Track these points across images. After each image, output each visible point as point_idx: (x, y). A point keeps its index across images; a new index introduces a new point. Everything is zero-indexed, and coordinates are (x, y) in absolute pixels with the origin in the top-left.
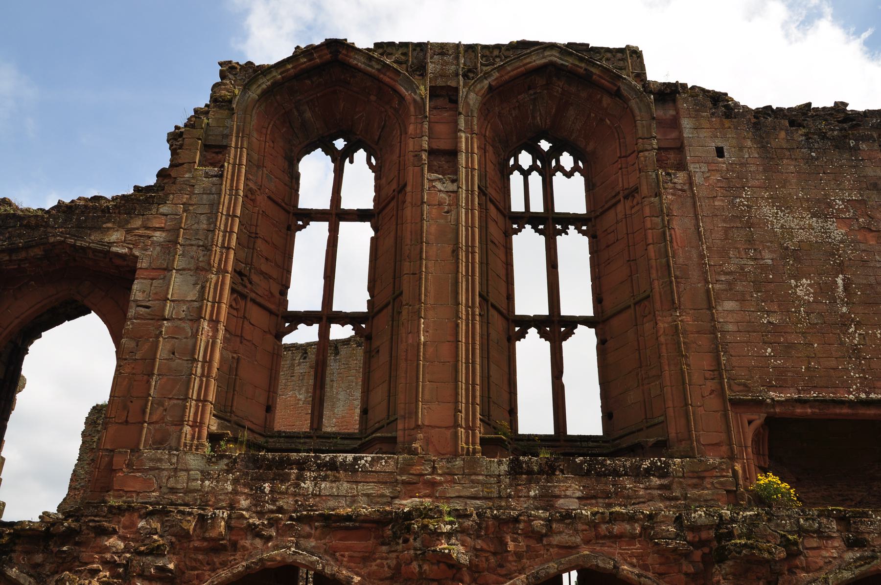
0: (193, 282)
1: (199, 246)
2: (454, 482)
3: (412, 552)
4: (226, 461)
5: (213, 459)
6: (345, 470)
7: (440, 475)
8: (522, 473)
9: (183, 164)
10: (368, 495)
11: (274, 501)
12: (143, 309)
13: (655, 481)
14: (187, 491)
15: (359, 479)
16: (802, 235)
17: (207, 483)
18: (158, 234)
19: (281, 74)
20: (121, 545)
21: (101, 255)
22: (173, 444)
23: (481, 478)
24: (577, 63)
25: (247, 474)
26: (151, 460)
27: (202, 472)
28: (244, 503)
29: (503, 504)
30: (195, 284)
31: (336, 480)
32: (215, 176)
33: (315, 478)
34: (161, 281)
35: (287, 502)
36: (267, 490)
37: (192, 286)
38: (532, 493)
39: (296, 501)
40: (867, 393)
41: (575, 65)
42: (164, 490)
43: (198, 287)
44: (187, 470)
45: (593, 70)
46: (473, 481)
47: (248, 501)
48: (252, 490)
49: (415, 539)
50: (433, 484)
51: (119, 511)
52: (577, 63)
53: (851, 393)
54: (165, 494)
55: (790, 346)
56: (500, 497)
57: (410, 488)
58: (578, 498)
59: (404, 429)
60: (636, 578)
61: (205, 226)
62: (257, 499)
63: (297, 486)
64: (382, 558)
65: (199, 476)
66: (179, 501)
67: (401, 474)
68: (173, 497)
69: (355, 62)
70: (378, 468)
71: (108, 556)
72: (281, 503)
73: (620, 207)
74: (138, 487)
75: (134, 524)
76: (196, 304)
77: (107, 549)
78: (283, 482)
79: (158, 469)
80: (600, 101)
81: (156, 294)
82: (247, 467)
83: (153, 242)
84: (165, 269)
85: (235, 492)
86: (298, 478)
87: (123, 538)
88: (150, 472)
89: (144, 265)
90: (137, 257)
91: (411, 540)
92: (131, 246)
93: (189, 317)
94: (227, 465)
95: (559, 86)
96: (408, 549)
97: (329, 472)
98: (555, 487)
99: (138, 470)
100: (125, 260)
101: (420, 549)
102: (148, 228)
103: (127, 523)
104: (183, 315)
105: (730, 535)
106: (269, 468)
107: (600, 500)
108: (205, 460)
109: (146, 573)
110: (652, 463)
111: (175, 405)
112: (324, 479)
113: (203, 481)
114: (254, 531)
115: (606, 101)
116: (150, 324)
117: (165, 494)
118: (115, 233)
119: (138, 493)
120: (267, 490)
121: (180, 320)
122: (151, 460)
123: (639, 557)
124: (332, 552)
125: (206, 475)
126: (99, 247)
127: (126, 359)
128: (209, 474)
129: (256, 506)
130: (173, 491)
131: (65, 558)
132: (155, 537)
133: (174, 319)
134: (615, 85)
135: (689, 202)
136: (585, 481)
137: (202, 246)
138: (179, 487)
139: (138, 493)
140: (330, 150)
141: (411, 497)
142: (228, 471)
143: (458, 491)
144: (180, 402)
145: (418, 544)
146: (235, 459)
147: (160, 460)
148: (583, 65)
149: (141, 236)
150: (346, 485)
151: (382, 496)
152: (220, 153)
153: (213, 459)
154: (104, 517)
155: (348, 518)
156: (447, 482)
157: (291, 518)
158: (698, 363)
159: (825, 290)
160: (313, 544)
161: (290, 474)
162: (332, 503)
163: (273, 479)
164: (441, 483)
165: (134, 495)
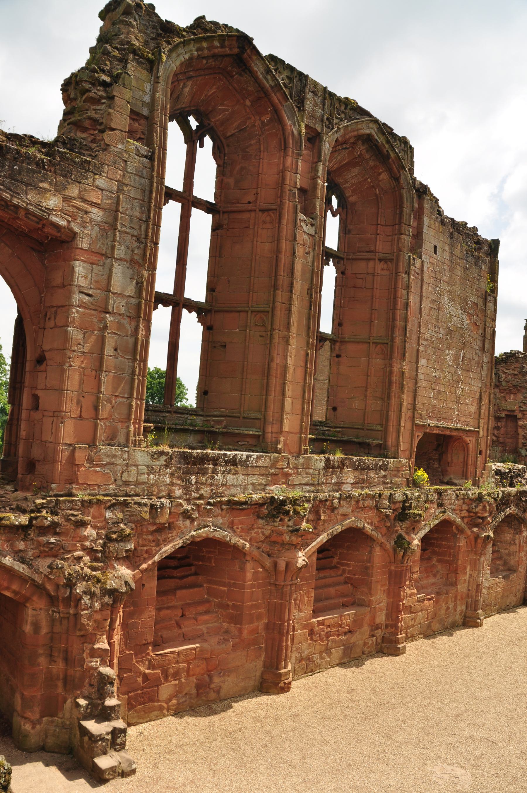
0: (130, 276)
1: (133, 236)
2: (298, 474)
3: (285, 528)
4: (164, 457)
5: (156, 456)
6: (241, 466)
7: (291, 469)
8: (330, 468)
9: (113, 129)
10: (253, 484)
11: (198, 490)
12: (87, 298)
13: (383, 473)
14: (138, 484)
15: (249, 472)
16: (455, 321)
17: (152, 476)
18: (95, 210)
19: (197, 50)
20: (94, 532)
21: (35, 219)
22: (121, 439)
23: (311, 471)
24: (384, 143)
25: (180, 468)
26: (108, 456)
27: (147, 467)
28: (178, 492)
29: (319, 488)
30: (132, 278)
31: (236, 473)
32: (146, 157)
33: (224, 472)
34: (101, 268)
35: (205, 491)
36: (193, 482)
37: (129, 280)
38: (333, 481)
39: (212, 490)
40: (457, 423)
41: (382, 143)
42: (119, 483)
43: (134, 282)
44: (136, 466)
45: (392, 155)
46: (307, 473)
47: (181, 491)
48: (183, 481)
49: (289, 520)
50: (287, 475)
51: (86, 505)
52: (384, 143)
53: (452, 423)
54: (120, 486)
55: (439, 392)
56: (318, 484)
57: (274, 479)
58: (352, 484)
59: (272, 433)
60: (370, 531)
61: (138, 214)
62: (187, 491)
63: (213, 478)
64: (258, 528)
65: (146, 471)
66: (132, 493)
67: (271, 468)
68: (128, 489)
69: (256, 69)
70: (259, 464)
71: (87, 544)
72: (201, 492)
73: (371, 264)
74: (99, 481)
75: (102, 515)
76: (134, 301)
77: (86, 538)
78: (203, 474)
79: (113, 464)
80: (380, 174)
81: (96, 282)
82: (180, 463)
83: (91, 219)
84: (103, 255)
85: (172, 484)
86: (213, 473)
87: (94, 527)
88: (108, 467)
89: (85, 246)
90: (75, 234)
91: (286, 520)
92: (70, 219)
93: (128, 314)
94: (166, 461)
95: (359, 148)
96: (283, 526)
97: (232, 467)
98: (343, 477)
99: (97, 465)
100: (59, 231)
101: (291, 527)
102: (85, 201)
103: (96, 514)
104: (123, 310)
105: (410, 508)
106: (194, 464)
107: (360, 485)
108: (149, 457)
109: (119, 556)
110: (383, 462)
111: (120, 403)
112: (229, 472)
113: (149, 475)
114: (186, 515)
115: (384, 176)
116: (93, 315)
117: (120, 486)
118: (53, 198)
119: (99, 486)
120: (193, 482)
121: (120, 315)
122: (108, 456)
123: (371, 518)
124: (231, 526)
125: (151, 470)
126: (38, 212)
127: (74, 351)
128: (153, 469)
129: (186, 494)
130: (126, 483)
131: (52, 548)
132: (122, 525)
133: (115, 313)
134: (399, 172)
135: (419, 282)
136: (357, 473)
137: (136, 236)
138: (131, 480)
139: (99, 486)
140: (185, 126)
141: (275, 484)
142: (166, 466)
143: (300, 480)
144: (125, 400)
145: (291, 523)
146: (171, 456)
147: (115, 456)
148: (387, 146)
149: (79, 209)
150: (242, 477)
151: (261, 484)
152: (137, 120)
153: (156, 456)
154: (78, 510)
155: (245, 503)
156: (294, 473)
157: (209, 504)
158: (407, 399)
159: (456, 358)
160: (221, 521)
161: (208, 469)
162: (233, 491)
163: (198, 473)
164: (290, 475)
165: (96, 488)
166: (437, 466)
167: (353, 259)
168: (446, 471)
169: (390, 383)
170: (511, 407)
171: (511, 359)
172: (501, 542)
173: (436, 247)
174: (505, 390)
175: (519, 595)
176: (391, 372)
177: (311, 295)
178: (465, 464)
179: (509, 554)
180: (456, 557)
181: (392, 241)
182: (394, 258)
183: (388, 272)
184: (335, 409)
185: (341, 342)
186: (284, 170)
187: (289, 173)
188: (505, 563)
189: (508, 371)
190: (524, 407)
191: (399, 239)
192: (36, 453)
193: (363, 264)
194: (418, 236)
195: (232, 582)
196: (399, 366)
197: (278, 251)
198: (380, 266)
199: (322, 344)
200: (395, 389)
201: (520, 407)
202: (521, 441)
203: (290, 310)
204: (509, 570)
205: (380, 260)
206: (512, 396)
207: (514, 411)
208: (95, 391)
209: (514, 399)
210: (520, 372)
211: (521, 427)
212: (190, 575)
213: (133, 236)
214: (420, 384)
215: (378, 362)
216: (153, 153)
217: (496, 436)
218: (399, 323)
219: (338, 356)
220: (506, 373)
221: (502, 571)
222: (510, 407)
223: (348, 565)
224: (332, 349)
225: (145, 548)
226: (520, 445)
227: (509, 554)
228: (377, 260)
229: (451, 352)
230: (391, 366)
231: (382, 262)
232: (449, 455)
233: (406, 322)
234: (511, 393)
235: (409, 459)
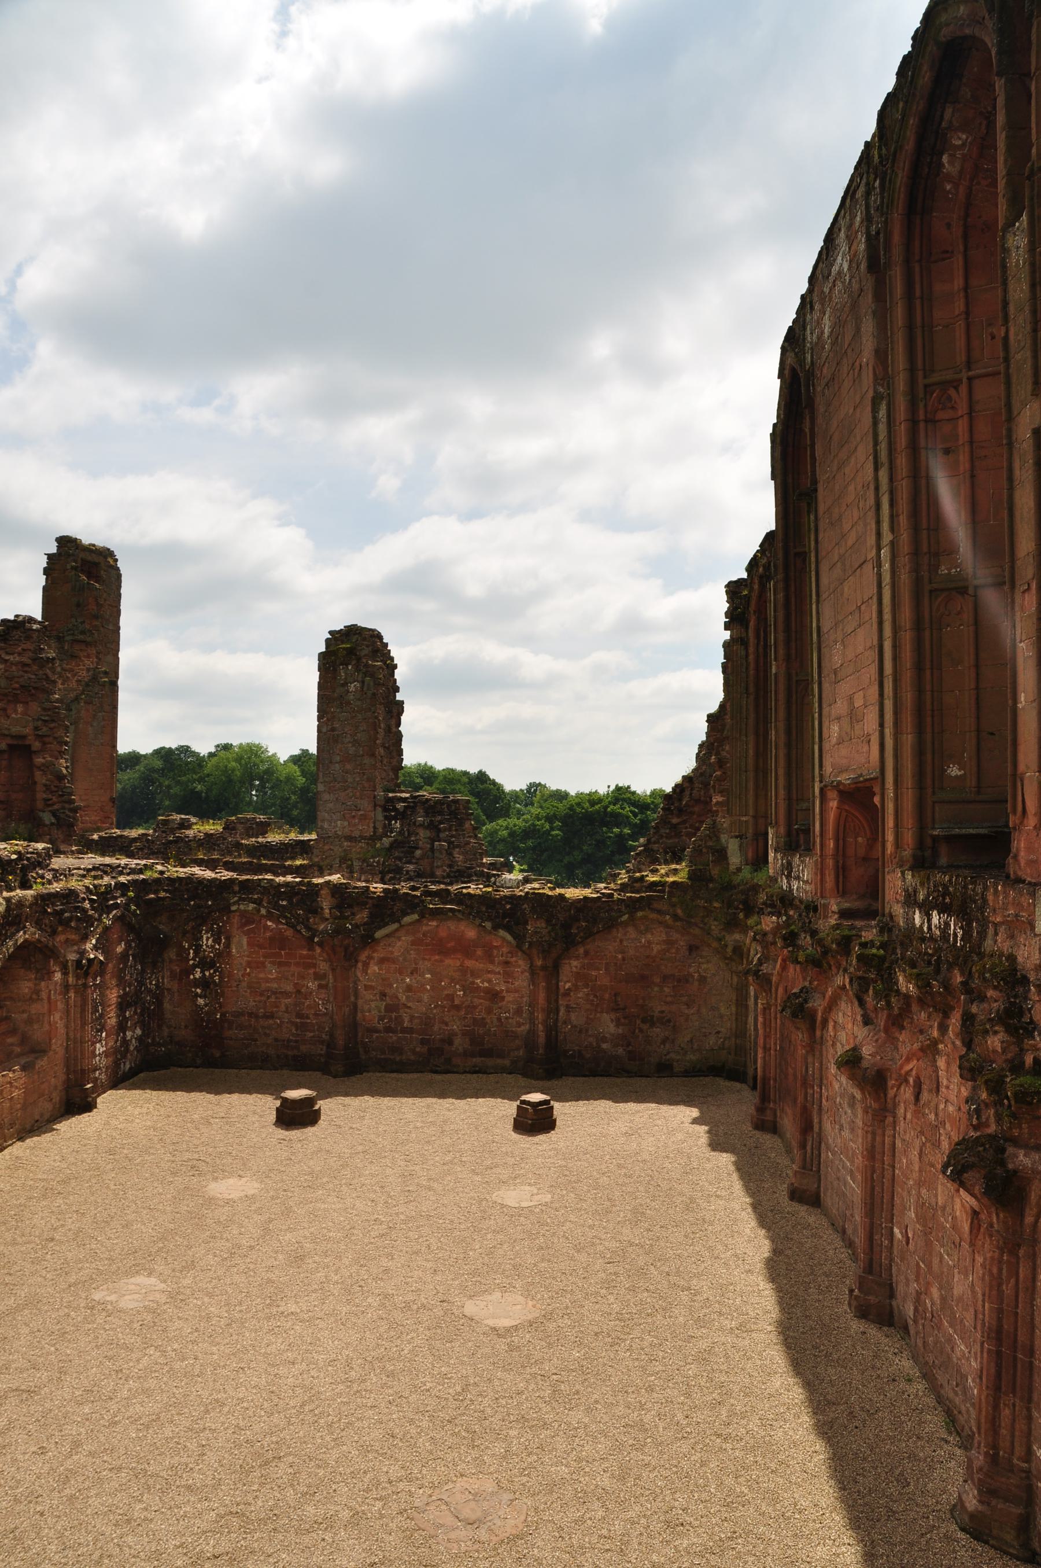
170: (18, 728)
171: (17, 634)
174: (5, 695)
175: (56, 1097)
179: (30, 1021)
188: (24, 1040)
189: (11, 658)
190: (45, 729)
202: (41, 795)
204: (33, 1051)
206: (20, 708)
207: (24, 737)
209: (24, 713)
210: (34, 660)
211: (39, 768)
220: (6, 661)
221: (18, 1056)
222: (15, 730)
226: (40, 804)
227: (30, 1021)
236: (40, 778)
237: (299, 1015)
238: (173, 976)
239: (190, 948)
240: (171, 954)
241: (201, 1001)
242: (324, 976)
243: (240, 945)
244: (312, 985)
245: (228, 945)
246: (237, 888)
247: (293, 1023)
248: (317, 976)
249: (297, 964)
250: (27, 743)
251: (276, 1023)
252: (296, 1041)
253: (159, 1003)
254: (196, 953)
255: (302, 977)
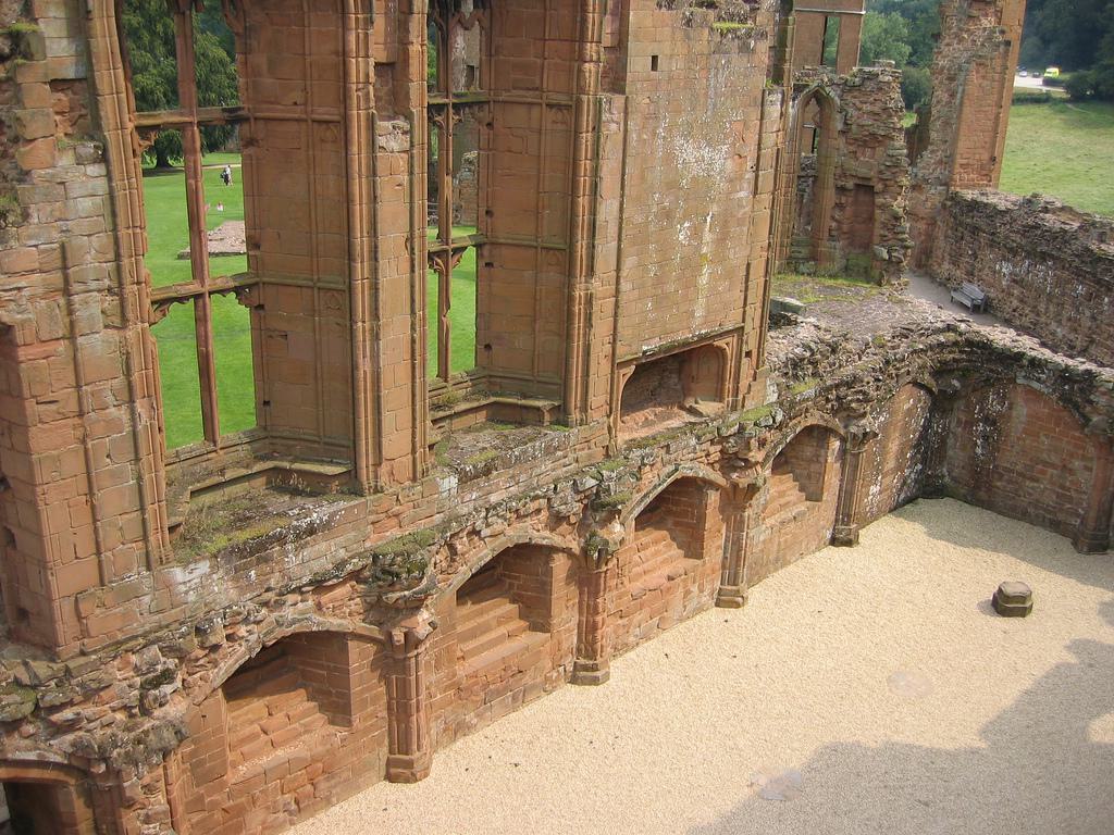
16: (696, 170)
73: (535, 112)
158: (601, 328)
159: (696, 233)
166: (676, 380)
167: (505, 102)
168: (690, 389)
169: (570, 314)
170: (864, 170)
171: (870, 85)
172: (797, 458)
173: (655, 58)
174: (856, 140)
176: (571, 299)
177: (412, 249)
178: (721, 379)
180: (702, 519)
181: (570, 71)
182: (573, 103)
183: (563, 127)
184: (488, 347)
185: (492, 244)
186: (344, 54)
187: (354, 60)
190: (888, 173)
191: (580, 71)
192: (27, 603)
193: (521, 111)
194: (620, 46)
195: (332, 665)
196: (583, 286)
197: (349, 200)
198: (551, 115)
199: (456, 257)
200: (578, 324)
201: (881, 172)
203: (377, 289)
205: (550, 106)
206: (868, 152)
207: (869, 179)
208: (91, 521)
211: (879, 207)
212: (273, 659)
213: (99, 291)
214: (623, 298)
215: (552, 276)
216: (105, 150)
217: (836, 221)
218: (583, 218)
219: (488, 265)
220: (860, 109)
222: (863, 171)
223: (516, 578)
224: (479, 256)
225: (198, 675)
226: (876, 239)
228: (544, 106)
229: (686, 225)
230: (571, 287)
231: (554, 110)
232: (694, 366)
233: (595, 215)
234: (865, 144)
235: (609, 416)
236: (880, 216)
237: (1062, 487)
238: (959, 422)
239: (977, 404)
240: (961, 404)
241: (979, 451)
242: (1091, 459)
243: (1022, 411)
244: (1077, 464)
245: (1010, 408)
246: (1025, 362)
247: (1054, 491)
248: (1084, 458)
249: (1068, 442)
250: (871, 184)
251: (1039, 487)
252: (1054, 508)
253: (943, 442)
254: (981, 410)
255: (1071, 455)
